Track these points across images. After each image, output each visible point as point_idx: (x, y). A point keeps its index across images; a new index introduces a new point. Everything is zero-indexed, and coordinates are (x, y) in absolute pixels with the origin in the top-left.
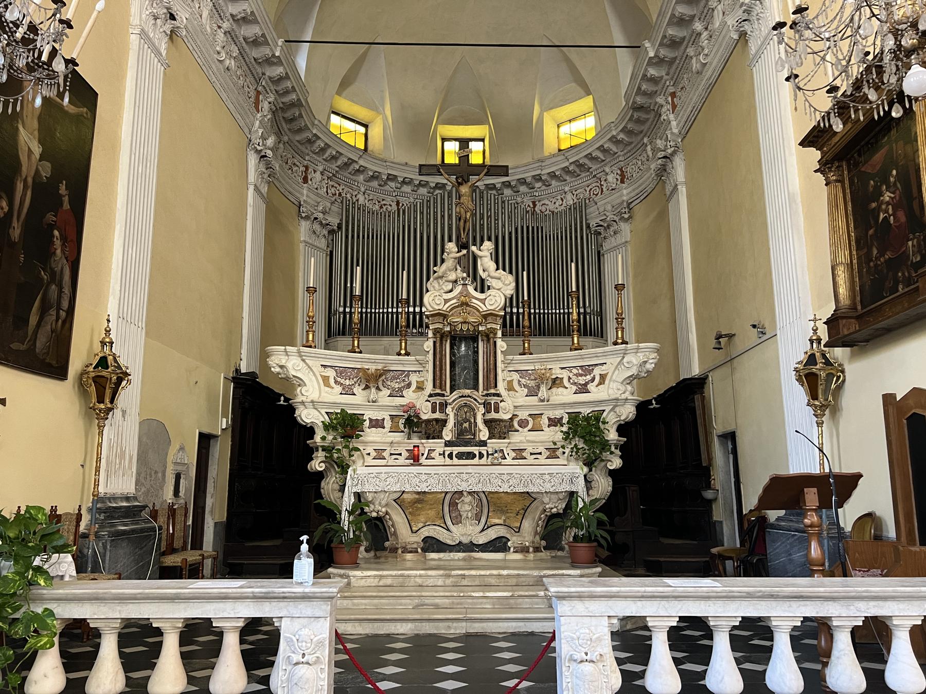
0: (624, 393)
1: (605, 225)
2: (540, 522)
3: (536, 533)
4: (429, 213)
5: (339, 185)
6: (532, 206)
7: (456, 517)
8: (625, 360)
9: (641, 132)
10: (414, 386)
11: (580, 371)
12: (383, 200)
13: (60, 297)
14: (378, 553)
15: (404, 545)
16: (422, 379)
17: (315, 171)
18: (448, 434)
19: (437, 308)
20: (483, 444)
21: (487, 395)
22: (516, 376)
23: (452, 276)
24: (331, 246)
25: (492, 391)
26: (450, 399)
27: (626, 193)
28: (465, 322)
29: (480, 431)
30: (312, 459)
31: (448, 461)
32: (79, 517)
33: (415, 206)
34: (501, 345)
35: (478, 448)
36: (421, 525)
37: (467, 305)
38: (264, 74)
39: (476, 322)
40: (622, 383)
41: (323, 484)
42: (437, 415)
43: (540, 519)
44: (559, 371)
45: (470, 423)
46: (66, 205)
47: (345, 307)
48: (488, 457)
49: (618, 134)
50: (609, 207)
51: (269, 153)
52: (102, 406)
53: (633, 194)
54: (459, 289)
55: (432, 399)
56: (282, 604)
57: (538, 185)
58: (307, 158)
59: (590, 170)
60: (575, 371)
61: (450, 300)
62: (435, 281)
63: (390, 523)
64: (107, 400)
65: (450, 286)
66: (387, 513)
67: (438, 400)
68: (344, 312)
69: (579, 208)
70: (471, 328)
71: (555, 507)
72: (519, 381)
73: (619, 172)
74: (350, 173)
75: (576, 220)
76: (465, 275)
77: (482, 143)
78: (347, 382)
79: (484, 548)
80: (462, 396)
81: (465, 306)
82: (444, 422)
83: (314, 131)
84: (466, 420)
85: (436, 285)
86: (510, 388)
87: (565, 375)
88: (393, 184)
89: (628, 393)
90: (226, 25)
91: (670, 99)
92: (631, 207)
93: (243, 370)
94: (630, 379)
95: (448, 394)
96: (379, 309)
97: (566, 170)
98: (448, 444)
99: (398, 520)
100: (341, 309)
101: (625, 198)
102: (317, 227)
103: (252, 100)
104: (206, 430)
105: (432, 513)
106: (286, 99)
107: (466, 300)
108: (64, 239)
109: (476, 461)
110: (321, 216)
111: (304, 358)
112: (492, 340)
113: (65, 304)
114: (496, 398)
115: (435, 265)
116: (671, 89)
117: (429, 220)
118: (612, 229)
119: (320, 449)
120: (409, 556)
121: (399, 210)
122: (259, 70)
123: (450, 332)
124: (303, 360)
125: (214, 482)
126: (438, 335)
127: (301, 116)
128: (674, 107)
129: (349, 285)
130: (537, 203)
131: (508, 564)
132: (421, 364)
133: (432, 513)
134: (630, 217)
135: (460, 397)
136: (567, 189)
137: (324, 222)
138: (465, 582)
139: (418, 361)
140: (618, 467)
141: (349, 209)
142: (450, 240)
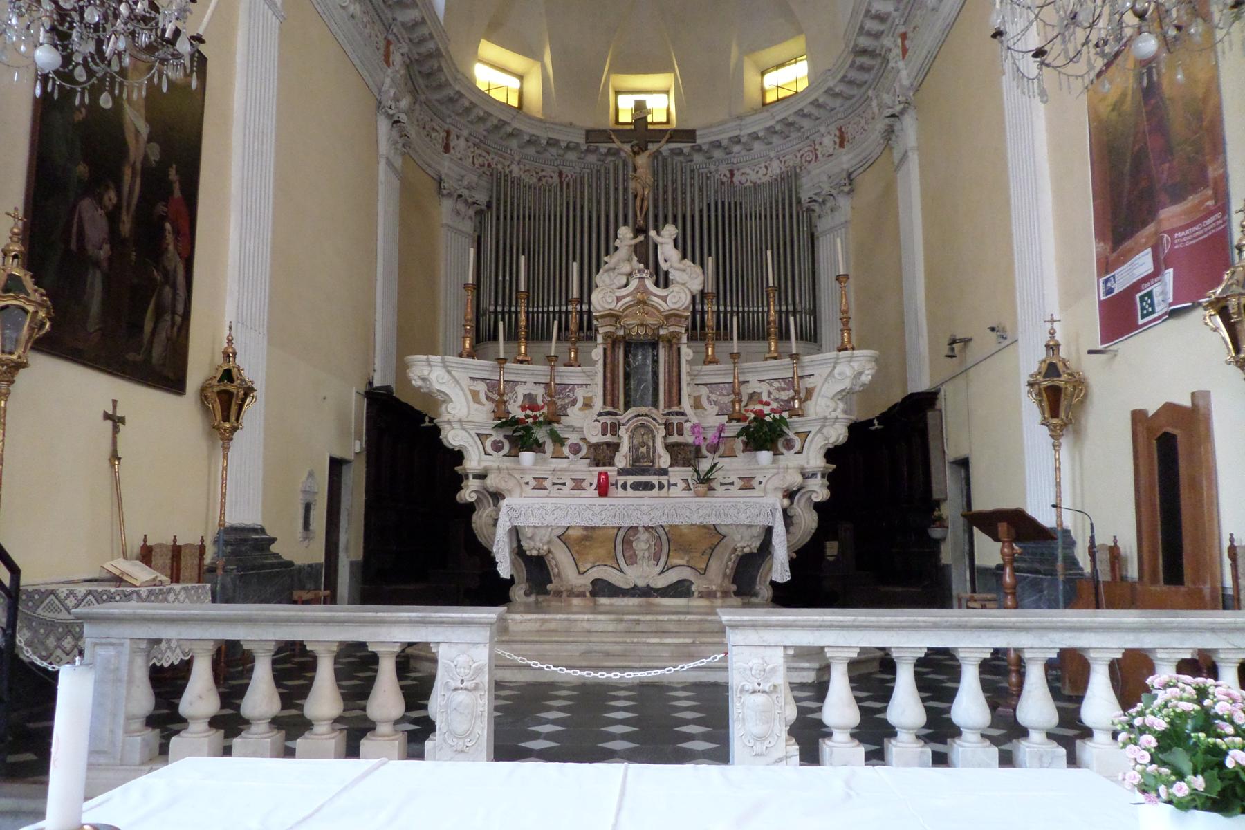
0: (835, 410)
1: (820, 200)
2: (730, 563)
3: (725, 575)
4: (598, 186)
5: (488, 153)
6: (729, 175)
7: (631, 557)
8: (836, 371)
9: (865, 82)
10: (580, 403)
11: (783, 385)
12: (542, 170)
13: (174, 299)
14: (541, 598)
15: (569, 588)
16: (590, 395)
17: (458, 137)
18: (621, 460)
19: (608, 307)
20: (664, 472)
21: (669, 414)
22: (704, 391)
23: (626, 268)
24: (479, 230)
25: (675, 409)
26: (624, 418)
27: (846, 160)
28: (642, 325)
29: (660, 457)
30: (462, 489)
32: (202, 549)
33: (582, 178)
34: (686, 352)
35: (657, 477)
36: (589, 566)
37: (645, 303)
38: (394, 19)
39: (656, 325)
40: (832, 399)
41: (475, 517)
42: (608, 438)
43: (730, 559)
44: (758, 384)
45: (648, 447)
46: (177, 193)
47: (496, 305)
48: (669, 488)
49: (835, 86)
50: (825, 178)
51: (403, 118)
52: (227, 425)
53: (854, 162)
55: (603, 419)
56: (439, 629)
57: (736, 148)
58: (448, 121)
59: (802, 130)
60: (776, 384)
61: (624, 297)
62: (605, 274)
63: (553, 563)
64: (233, 418)
65: (624, 281)
66: (550, 551)
67: (608, 419)
68: (496, 312)
69: (790, 179)
70: (650, 332)
71: (748, 546)
72: (708, 397)
73: (837, 133)
74: (501, 138)
75: (783, 193)
76: (642, 266)
77: (665, 96)
79: (665, 592)
80: (639, 415)
81: (641, 305)
82: (615, 447)
83: (457, 88)
84: (643, 444)
85: (608, 281)
86: (697, 405)
88: (553, 151)
89: (839, 410)
91: (899, 41)
92: (852, 177)
93: (377, 383)
94: (845, 395)
96: (538, 307)
97: (771, 131)
98: (622, 472)
99: (563, 562)
100: (492, 308)
101: (845, 166)
102: (461, 207)
103: (382, 51)
104: (338, 454)
105: (602, 552)
106: (423, 50)
107: (643, 297)
108: (177, 232)
109: (655, 492)
110: (465, 193)
111: (450, 369)
112: (675, 346)
113: (180, 308)
114: (680, 417)
115: (607, 253)
116: (902, 29)
117: (599, 195)
118: (829, 205)
119: (471, 477)
120: (576, 601)
121: (561, 183)
122: (390, 15)
123: (624, 337)
124: (449, 372)
125: (348, 515)
126: (609, 340)
127: (440, 69)
128: (905, 51)
129: (500, 278)
130: (735, 172)
131: (690, 610)
132: (588, 376)
133: (602, 552)
134: (851, 191)
135: (636, 416)
136: (772, 154)
137: (470, 200)
138: (639, 628)
139: (584, 372)
140: (824, 500)
141: (499, 181)
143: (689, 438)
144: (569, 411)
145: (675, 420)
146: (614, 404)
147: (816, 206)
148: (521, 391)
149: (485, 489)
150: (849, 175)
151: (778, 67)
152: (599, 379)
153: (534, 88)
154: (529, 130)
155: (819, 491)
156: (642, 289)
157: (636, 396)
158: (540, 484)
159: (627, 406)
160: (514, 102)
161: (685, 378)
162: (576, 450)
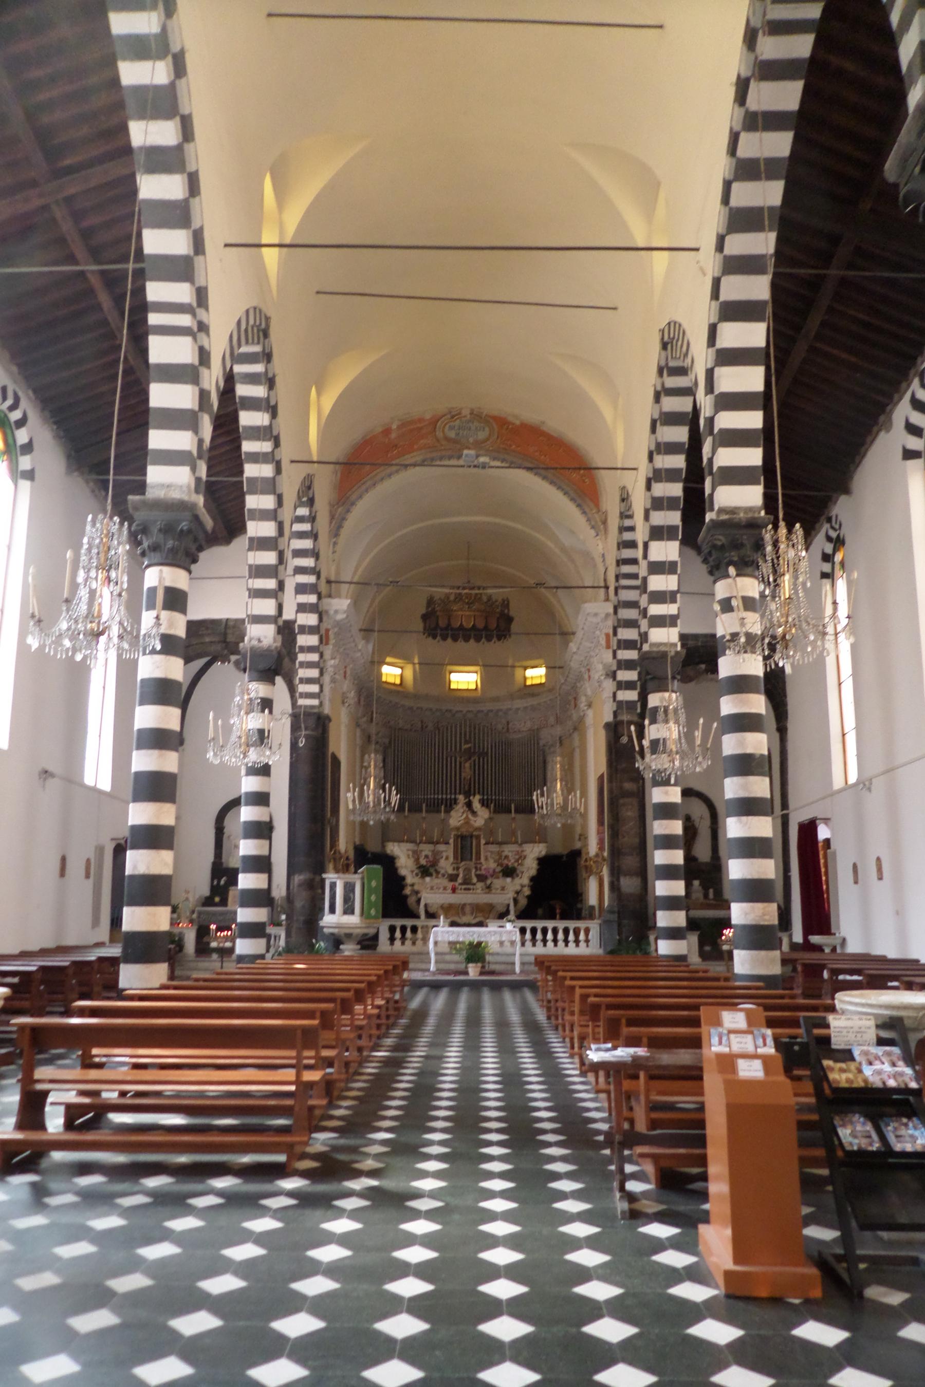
10: (444, 858)
18: (460, 880)
23: (462, 811)
27: (558, 731)
34: (483, 841)
41: (409, 899)
42: (455, 872)
54: (465, 815)
69: (534, 734)
82: (458, 875)
86: (486, 859)
87: (510, 854)
90: (356, 682)
93: (358, 843)
95: (459, 861)
97: (526, 708)
98: (460, 884)
109: (471, 891)
110: (380, 740)
142: (460, 793)
143: (483, 872)
145: (479, 866)
146: (457, 859)
148: (424, 854)
150: (560, 738)
151: (533, 667)
152: (452, 850)
153: (409, 673)
154: (408, 703)
155: (527, 891)
156: (467, 817)
158: (432, 888)
159: (462, 861)
161: (482, 849)
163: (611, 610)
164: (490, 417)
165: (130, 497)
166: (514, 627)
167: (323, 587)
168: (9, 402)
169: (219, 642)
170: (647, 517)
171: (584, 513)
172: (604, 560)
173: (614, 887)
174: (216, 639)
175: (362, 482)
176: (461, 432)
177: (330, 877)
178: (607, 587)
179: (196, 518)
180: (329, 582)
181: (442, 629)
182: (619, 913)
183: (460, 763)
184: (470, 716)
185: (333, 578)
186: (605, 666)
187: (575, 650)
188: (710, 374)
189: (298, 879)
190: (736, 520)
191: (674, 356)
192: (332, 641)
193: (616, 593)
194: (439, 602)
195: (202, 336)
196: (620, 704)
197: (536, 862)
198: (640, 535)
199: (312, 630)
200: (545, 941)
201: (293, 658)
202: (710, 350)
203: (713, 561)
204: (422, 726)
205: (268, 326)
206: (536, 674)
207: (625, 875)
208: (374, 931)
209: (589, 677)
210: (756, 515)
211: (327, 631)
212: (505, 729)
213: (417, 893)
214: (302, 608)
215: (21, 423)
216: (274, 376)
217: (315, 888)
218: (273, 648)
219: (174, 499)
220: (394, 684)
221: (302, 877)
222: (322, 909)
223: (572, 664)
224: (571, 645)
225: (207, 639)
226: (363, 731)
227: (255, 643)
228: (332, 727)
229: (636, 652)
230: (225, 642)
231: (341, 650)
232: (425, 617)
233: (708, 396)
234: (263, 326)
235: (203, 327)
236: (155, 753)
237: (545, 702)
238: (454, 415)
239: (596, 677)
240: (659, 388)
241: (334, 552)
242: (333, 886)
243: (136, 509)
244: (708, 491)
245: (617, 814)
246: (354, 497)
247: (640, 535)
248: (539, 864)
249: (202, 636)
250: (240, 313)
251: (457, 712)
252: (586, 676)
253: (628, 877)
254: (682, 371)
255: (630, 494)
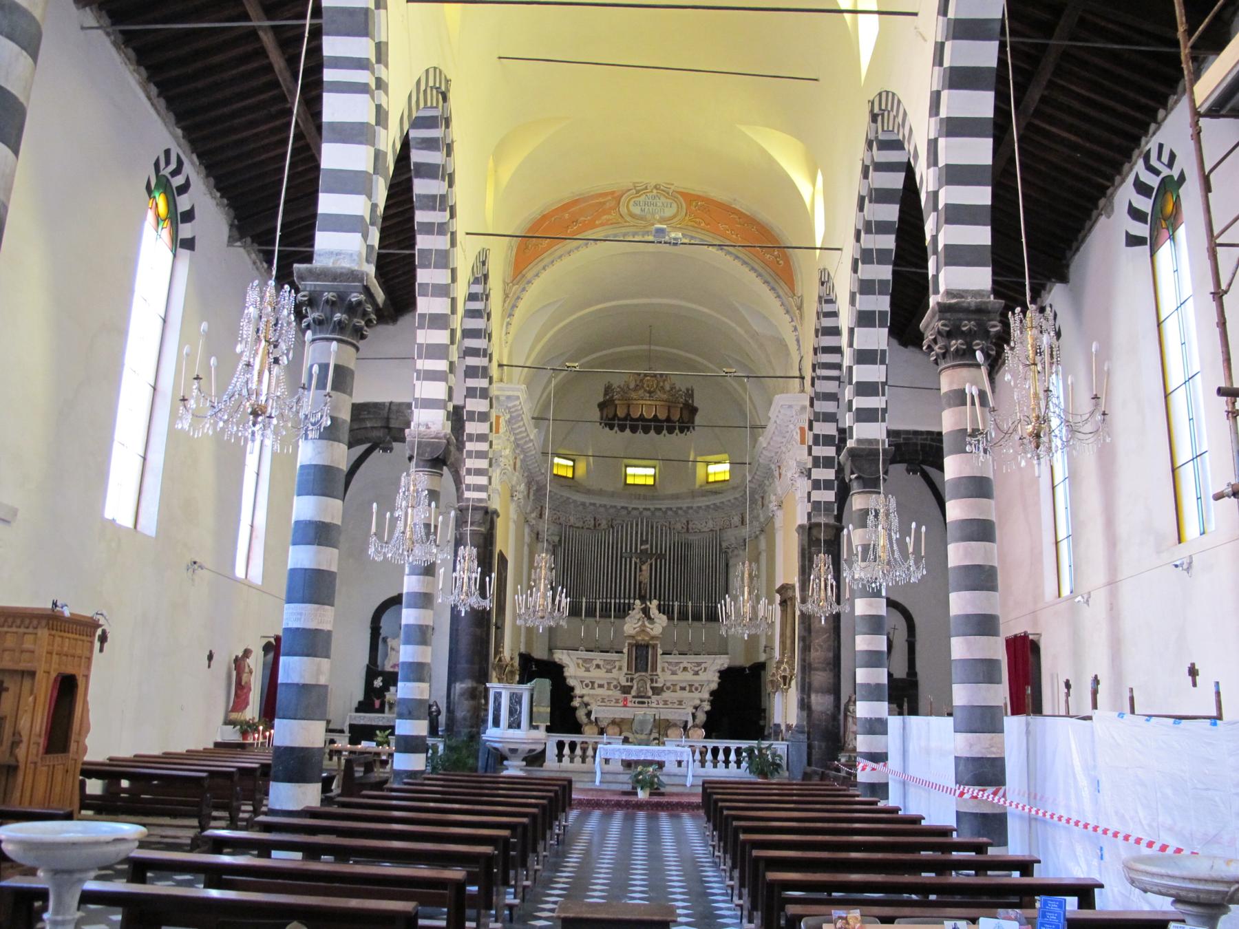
10: (617, 668)
18: (633, 692)
20: (649, 697)
22: (666, 665)
23: (638, 617)
27: (746, 531)
30: (572, 701)
31: (634, 705)
34: (660, 651)
41: (577, 712)
42: (629, 684)
50: (733, 538)
54: (640, 623)
57: (690, 511)
67: (629, 676)
69: (717, 534)
78: (588, 666)
82: (631, 687)
86: (663, 670)
87: (689, 666)
88: (592, 507)
90: (526, 474)
93: (523, 650)
97: (708, 506)
98: (634, 697)
109: (646, 705)
136: (709, 517)
144: (613, 671)
145: (655, 677)
146: (631, 670)
147: (729, 551)
149: (583, 702)
151: (716, 463)
155: (707, 707)
156: (643, 625)
157: (639, 666)
160: (570, 475)
162: (615, 687)
163: (808, 403)
164: (678, 192)
165: (296, 265)
166: (698, 419)
167: (494, 371)
168: (173, 166)
169: (381, 427)
170: (853, 302)
171: (779, 297)
172: (799, 349)
173: (805, 705)
174: (379, 424)
175: (538, 259)
176: (647, 208)
177: (494, 686)
178: (803, 378)
179: (367, 290)
180: (500, 366)
181: (619, 419)
182: (809, 733)
183: (636, 563)
184: (648, 513)
185: (505, 363)
186: (799, 463)
187: (765, 445)
188: (933, 145)
189: (459, 687)
190: (965, 305)
191: (885, 128)
192: (502, 430)
193: (813, 385)
194: (618, 389)
195: (380, 95)
196: (816, 505)
197: (718, 674)
198: (845, 320)
199: (483, 417)
200: (727, 762)
201: (460, 446)
202: (933, 120)
203: (939, 348)
204: (595, 526)
205: (448, 89)
206: (719, 471)
207: (817, 692)
208: (542, 747)
209: (780, 474)
210: (985, 300)
211: (498, 418)
212: (685, 530)
213: (587, 705)
214: (471, 393)
215: (183, 189)
216: (453, 142)
217: (478, 696)
218: (442, 435)
219: (342, 268)
220: (565, 477)
221: (463, 685)
222: (485, 721)
223: (761, 461)
224: (761, 439)
225: (369, 425)
226: (532, 527)
227: (422, 429)
228: (499, 522)
229: (835, 448)
230: (388, 428)
231: (512, 439)
232: (602, 406)
233: (932, 169)
234: (443, 89)
235: (380, 84)
236: (315, 547)
237: (729, 501)
238: (639, 190)
239: (789, 475)
240: (868, 162)
241: (507, 333)
242: (498, 696)
243: (302, 278)
244: (931, 271)
245: (810, 625)
246: (529, 275)
247: (845, 320)
248: (720, 678)
249: (363, 420)
250: (420, 73)
251: (634, 509)
252: (776, 474)
253: (820, 694)
254: (898, 145)
255: (832, 275)
